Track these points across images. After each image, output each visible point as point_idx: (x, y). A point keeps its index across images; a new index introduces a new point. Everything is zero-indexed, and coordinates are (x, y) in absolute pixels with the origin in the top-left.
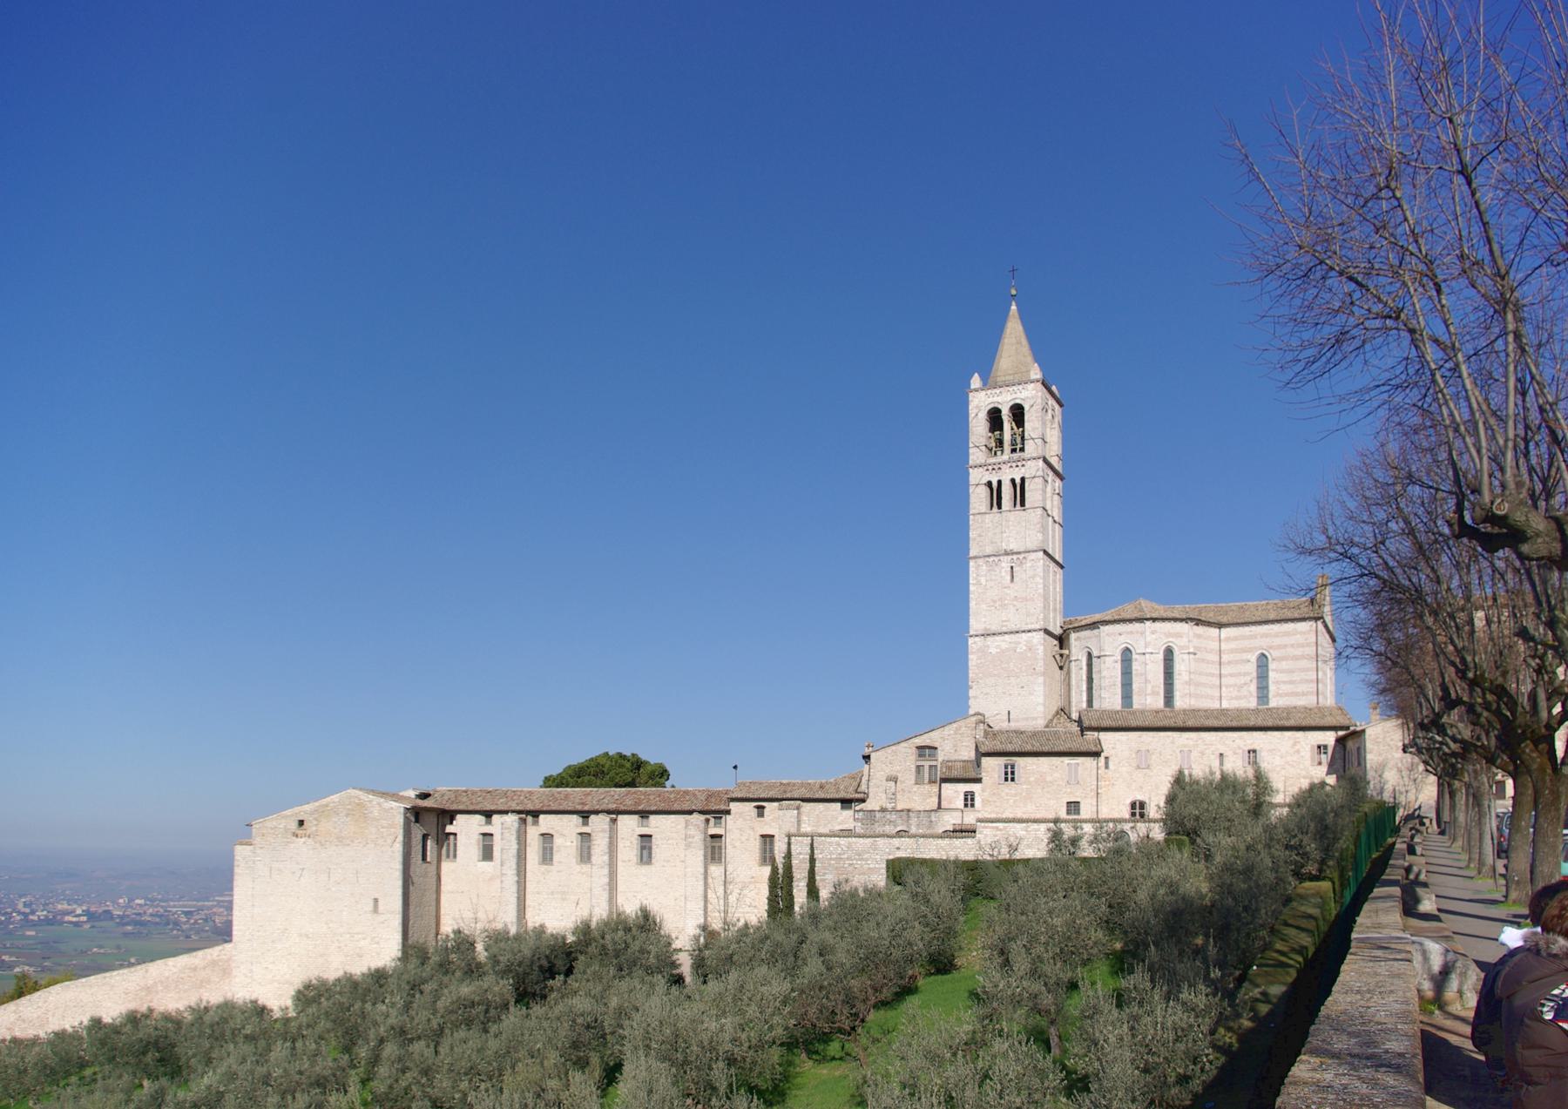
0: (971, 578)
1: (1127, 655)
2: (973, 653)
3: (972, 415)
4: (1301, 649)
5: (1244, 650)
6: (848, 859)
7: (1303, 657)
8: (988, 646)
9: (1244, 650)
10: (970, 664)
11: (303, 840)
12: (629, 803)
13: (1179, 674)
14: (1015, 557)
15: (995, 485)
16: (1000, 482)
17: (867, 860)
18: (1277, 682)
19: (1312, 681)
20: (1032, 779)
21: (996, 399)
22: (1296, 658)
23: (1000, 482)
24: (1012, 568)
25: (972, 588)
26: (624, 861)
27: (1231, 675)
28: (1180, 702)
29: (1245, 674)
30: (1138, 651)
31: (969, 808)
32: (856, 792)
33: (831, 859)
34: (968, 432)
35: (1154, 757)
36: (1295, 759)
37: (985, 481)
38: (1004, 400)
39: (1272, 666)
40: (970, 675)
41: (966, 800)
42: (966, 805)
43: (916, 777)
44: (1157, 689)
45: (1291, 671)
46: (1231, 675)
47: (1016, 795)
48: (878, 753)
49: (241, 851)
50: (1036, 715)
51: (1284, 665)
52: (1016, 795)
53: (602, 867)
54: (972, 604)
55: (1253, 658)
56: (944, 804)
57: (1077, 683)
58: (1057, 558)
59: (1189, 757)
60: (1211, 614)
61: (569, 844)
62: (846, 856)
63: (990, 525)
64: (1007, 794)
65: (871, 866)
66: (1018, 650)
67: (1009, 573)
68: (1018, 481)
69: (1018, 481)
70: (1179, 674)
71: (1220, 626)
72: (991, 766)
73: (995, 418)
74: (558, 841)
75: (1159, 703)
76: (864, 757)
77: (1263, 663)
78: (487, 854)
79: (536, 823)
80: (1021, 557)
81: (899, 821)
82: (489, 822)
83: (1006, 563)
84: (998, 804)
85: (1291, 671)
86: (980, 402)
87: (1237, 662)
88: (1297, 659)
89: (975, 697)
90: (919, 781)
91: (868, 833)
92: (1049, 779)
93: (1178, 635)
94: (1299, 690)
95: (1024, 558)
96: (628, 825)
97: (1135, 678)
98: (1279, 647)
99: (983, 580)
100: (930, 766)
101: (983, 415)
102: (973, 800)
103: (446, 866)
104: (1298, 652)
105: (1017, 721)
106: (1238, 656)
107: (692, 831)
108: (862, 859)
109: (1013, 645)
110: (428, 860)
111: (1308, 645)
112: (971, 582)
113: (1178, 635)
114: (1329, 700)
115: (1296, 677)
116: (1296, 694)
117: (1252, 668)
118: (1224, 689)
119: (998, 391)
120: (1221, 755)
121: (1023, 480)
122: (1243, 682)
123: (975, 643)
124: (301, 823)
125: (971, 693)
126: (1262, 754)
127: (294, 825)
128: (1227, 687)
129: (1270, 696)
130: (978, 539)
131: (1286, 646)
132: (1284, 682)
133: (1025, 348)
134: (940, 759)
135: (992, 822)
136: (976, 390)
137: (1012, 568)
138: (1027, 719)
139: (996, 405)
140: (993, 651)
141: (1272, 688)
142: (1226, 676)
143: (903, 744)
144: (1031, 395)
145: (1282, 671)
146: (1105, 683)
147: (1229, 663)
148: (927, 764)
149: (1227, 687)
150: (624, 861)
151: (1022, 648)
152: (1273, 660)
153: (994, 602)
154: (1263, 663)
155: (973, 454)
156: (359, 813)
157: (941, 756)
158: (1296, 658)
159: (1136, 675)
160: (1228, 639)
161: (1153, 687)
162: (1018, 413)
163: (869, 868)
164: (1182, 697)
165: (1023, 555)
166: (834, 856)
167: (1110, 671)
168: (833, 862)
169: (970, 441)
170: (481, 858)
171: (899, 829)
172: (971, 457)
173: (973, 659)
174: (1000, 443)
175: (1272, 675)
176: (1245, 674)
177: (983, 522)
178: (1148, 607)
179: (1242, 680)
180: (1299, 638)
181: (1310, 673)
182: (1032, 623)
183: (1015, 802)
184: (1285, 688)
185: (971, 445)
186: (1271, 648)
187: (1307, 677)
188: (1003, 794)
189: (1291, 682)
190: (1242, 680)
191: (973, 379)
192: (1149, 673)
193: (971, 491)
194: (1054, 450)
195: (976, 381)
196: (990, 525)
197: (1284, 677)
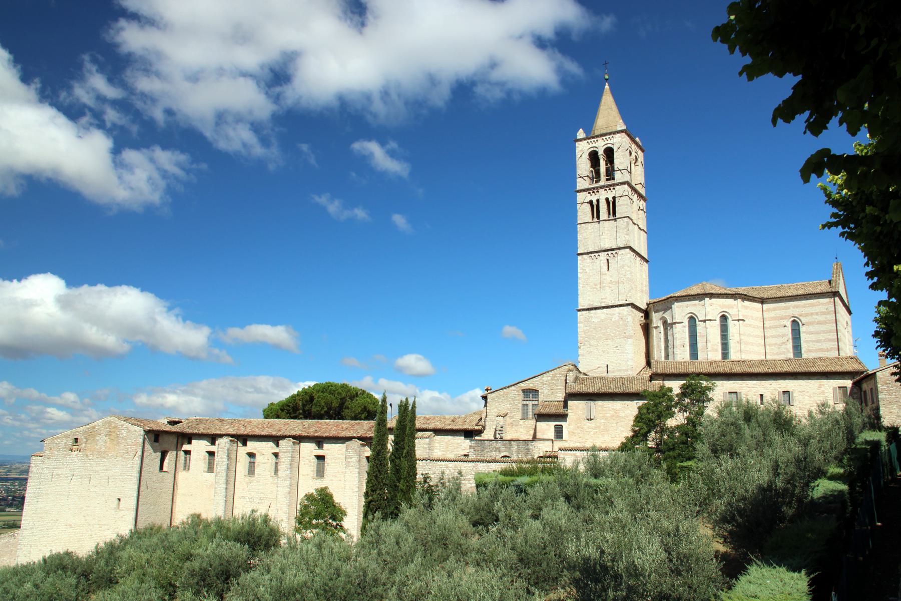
0: (579, 269)
1: (692, 320)
2: (581, 322)
3: (578, 156)
4: (824, 316)
5: (782, 318)
7: (825, 323)
8: (592, 317)
9: (782, 318)
10: (579, 330)
11: (76, 452)
12: (311, 432)
13: (733, 336)
14: (609, 253)
15: (595, 203)
16: (598, 201)
20: (608, 415)
21: (594, 145)
22: (819, 323)
23: (598, 201)
24: (608, 260)
25: (579, 275)
26: (303, 475)
27: (773, 337)
28: (733, 355)
29: (783, 336)
32: (477, 425)
34: (576, 168)
38: (600, 145)
39: (802, 329)
40: (579, 339)
44: (715, 347)
45: (818, 333)
46: (773, 337)
47: (595, 428)
48: (493, 395)
49: (35, 461)
51: (812, 328)
52: (595, 428)
53: (285, 480)
54: (580, 287)
55: (789, 324)
56: (539, 436)
57: (658, 344)
58: (643, 254)
61: (266, 461)
64: (588, 428)
66: (613, 320)
67: (606, 264)
68: (611, 199)
69: (611, 199)
70: (733, 336)
71: (762, 301)
72: (576, 408)
73: (594, 157)
74: (258, 458)
75: (718, 357)
77: (796, 325)
78: (211, 468)
79: (245, 444)
80: (614, 252)
81: (503, 449)
82: (213, 443)
84: (581, 435)
85: (818, 333)
86: (583, 149)
87: (776, 327)
88: (821, 324)
89: (583, 355)
92: (623, 415)
93: (731, 307)
95: (616, 253)
96: (309, 449)
97: (698, 339)
98: (807, 315)
99: (588, 270)
100: (533, 405)
101: (586, 156)
103: (182, 475)
104: (822, 318)
105: (613, 372)
106: (777, 322)
107: (351, 453)
110: (165, 469)
111: (829, 313)
112: (579, 271)
113: (731, 307)
114: (848, 350)
115: (822, 337)
117: (788, 331)
118: (767, 347)
119: (595, 140)
121: (614, 198)
122: (782, 341)
123: (582, 315)
124: (76, 440)
125: (580, 352)
126: (794, 395)
127: (70, 442)
128: (770, 345)
129: (803, 352)
131: (812, 314)
134: (540, 400)
135: (570, 450)
136: (581, 140)
137: (608, 260)
138: (620, 371)
139: (594, 149)
140: (595, 320)
141: (803, 345)
142: (768, 337)
143: (513, 388)
144: (620, 143)
145: (811, 333)
147: (770, 328)
149: (770, 345)
150: (303, 475)
151: (616, 318)
152: (803, 325)
153: (596, 285)
154: (796, 325)
156: (112, 433)
157: (541, 397)
158: (819, 323)
160: (768, 310)
161: (712, 345)
162: (609, 152)
164: (734, 353)
165: (615, 251)
167: (681, 333)
169: (577, 173)
170: (206, 469)
171: (503, 454)
172: (578, 184)
173: (581, 327)
174: (598, 173)
175: (803, 336)
176: (783, 336)
177: (587, 229)
178: (710, 288)
179: (780, 340)
180: (823, 309)
181: (832, 334)
183: (594, 434)
185: (578, 176)
186: (801, 315)
187: (829, 337)
188: (585, 427)
189: (818, 341)
190: (780, 340)
191: (579, 132)
192: (710, 335)
193: (578, 207)
194: (638, 176)
195: (581, 134)
197: (813, 337)
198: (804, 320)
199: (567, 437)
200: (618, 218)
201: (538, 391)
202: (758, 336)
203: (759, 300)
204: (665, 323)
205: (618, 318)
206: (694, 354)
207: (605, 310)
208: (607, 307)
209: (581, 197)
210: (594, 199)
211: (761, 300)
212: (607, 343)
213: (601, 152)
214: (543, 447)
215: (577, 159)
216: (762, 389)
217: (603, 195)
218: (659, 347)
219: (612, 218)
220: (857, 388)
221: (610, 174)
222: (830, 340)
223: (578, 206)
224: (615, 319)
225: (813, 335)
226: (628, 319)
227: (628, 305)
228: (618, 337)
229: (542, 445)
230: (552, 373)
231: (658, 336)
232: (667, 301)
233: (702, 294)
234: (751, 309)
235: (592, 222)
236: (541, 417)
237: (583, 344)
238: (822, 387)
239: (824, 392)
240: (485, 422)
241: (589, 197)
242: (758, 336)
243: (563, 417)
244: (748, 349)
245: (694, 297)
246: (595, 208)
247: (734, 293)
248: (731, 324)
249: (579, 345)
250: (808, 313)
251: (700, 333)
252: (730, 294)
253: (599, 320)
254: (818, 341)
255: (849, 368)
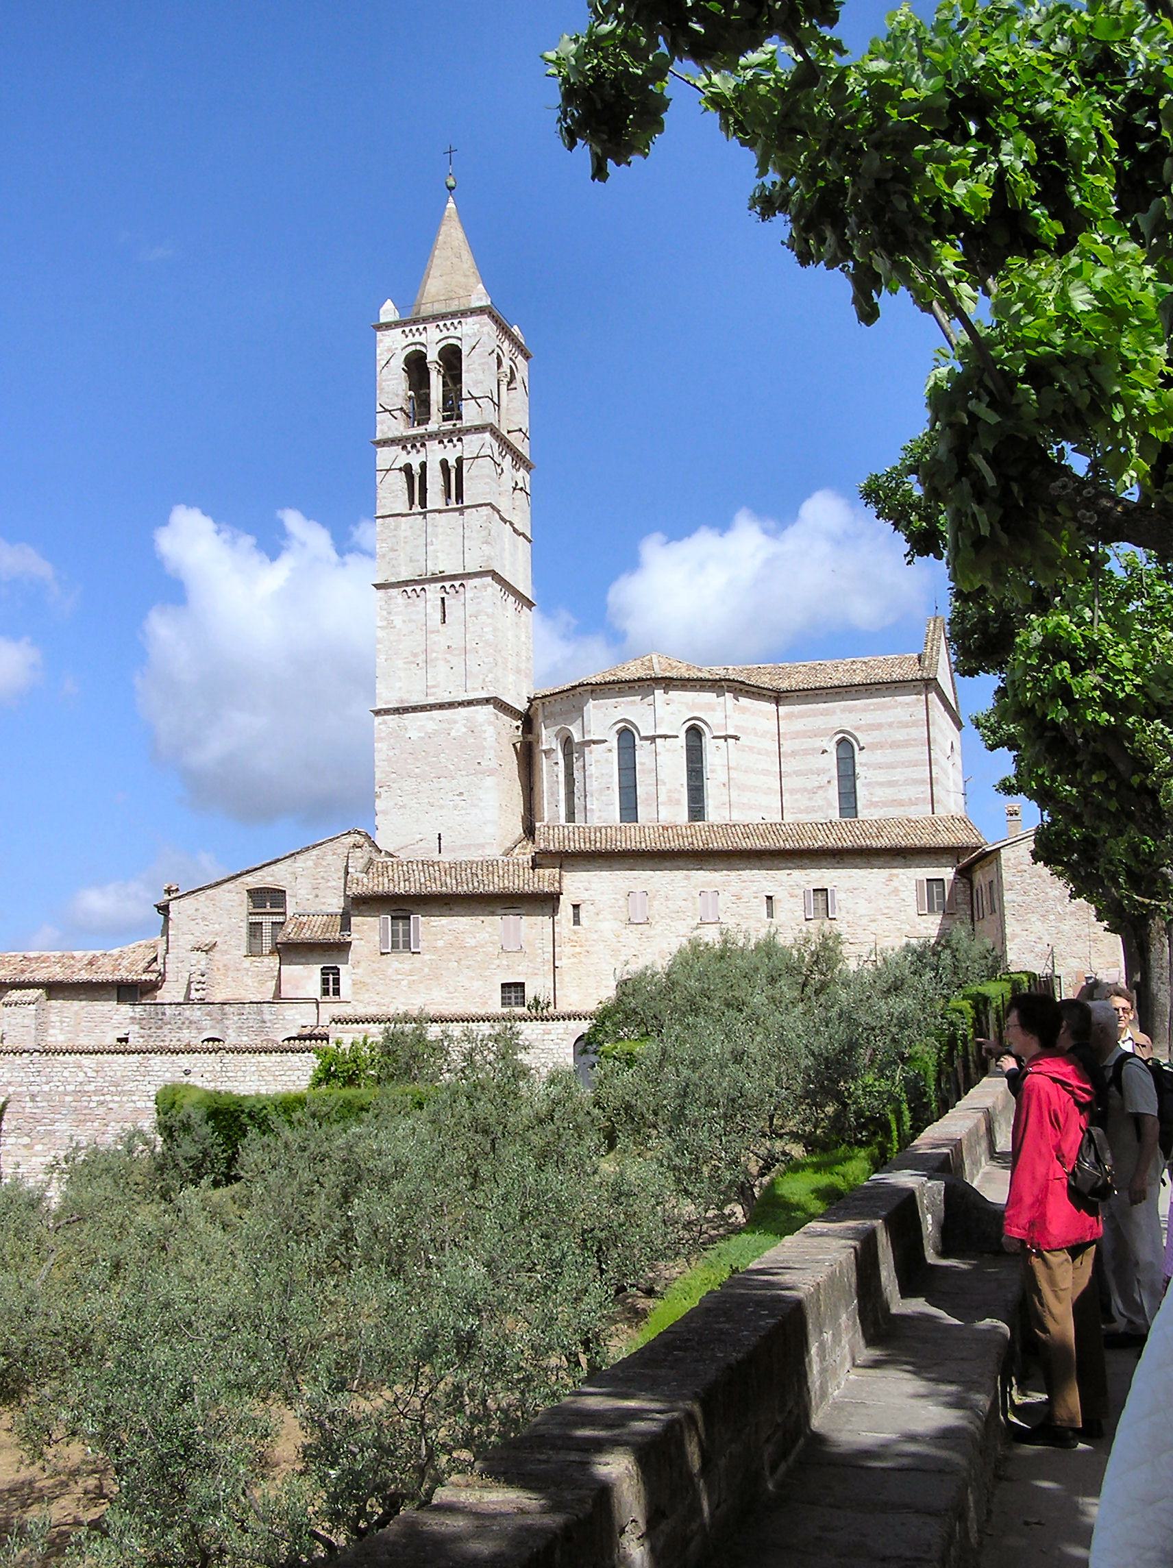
1: (627, 736)
2: (381, 739)
5: (816, 734)
6: (95, 1092)
9: (816, 734)
14: (447, 584)
15: (416, 469)
16: (423, 466)
17: (131, 1093)
18: (869, 784)
19: (922, 782)
21: (418, 338)
22: (895, 745)
23: (423, 466)
24: (443, 599)
27: (798, 773)
30: (642, 734)
31: (331, 997)
32: (146, 971)
33: (66, 1094)
35: (656, 903)
36: (891, 904)
37: (400, 464)
38: (432, 341)
39: (859, 757)
40: (377, 776)
41: (325, 982)
42: (325, 992)
43: (250, 944)
44: (676, 796)
45: (891, 766)
46: (798, 773)
50: (482, 841)
51: (878, 756)
55: (832, 747)
56: (286, 991)
57: (551, 788)
59: (716, 903)
60: (766, 679)
62: (91, 1087)
63: (408, 533)
65: (139, 1104)
66: (453, 733)
68: (452, 463)
69: (452, 463)
70: (712, 771)
71: (778, 697)
73: (416, 365)
76: (159, 908)
77: (846, 747)
81: (207, 1023)
83: (433, 591)
84: (380, 988)
85: (891, 766)
87: (806, 752)
89: (385, 812)
90: (253, 952)
91: (151, 1044)
92: (471, 942)
94: (904, 796)
99: (398, 621)
101: (398, 363)
102: (336, 981)
104: (900, 735)
108: (119, 1093)
109: (446, 725)
111: (915, 724)
113: (710, 708)
114: (952, 803)
115: (898, 775)
116: (900, 803)
117: (831, 761)
119: (421, 327)
120: (769, 898)
121: (460, 461)
125: (379, 805)
126: (837, 896)
130: (391, 555)
132: (881, 784)
133: (467, 261)
134: (290, 913)
136: (388, 326)
137: (443, 599)
139: (419, 347)
140: (414, 735)
142: (789, 775)
146: (593, 785)
147: (794, 754)
148: (267, 920)
151: (459, 730)
152: (862, 749)
153: (415, 655)
154: (846, 747)
155: (383, 422)
158: (895, 745)
159: (643, 771)
160: (790, 716)
162: (452, 358)
163: (136, 1110)
166: (70, 1088)
168: (69, 1099)
179: (814, 781)
182: (475, 689)
184: (881, 794)
186: (857, 729)
189: (891, 784)
193: (378, 479)
195: (388, 312)
196: (408, 533)
197: (881, 776)
198: (863, 739)
199: (350, 992)
200: (468, 507)
201: (284, 892)
202: (766, 772)
203: (770, 693)
204: (567, 742)
205: (464, 730)
206: (629, 809)
207: (435, 713)
208: (441, 706)
209: (385, 456)
210: (415, 460)
211: (775, 694)
212: (441, 785)
213: (432, 356)
214: (296, 1017)
215: (378, 369)
216: (771, 884)
217: (435, 453)
218: (554, 794)
219: (456, 506)
220: (965, 880)
221: (452, 409)
222: (916, 782)
223: (379, 476)
224: (458, 731)
225: (882, 771)
226: (485, 732)
227: (487, 701)
228: (464, 773)
229: (294, 1011)
230: (315, 852)
231: (551, 773)
232: (572, 692)
233: (647, 679)
234: (754, 714)
235: (409, 515)
236: (291, 951)
237: (386, 788)
238: (895, 878)
239: (898, 890)
240: (164, 963)
241: (403, 458)
242: (766, 772)
243: (342, 948)
244: (745, 801)
245: (631, 685)
246: (416, 482)
247: (717, 677)
248: (709, 744)
249: (377, 789)
250: (873, 725)
251: (644, 764)
252: (709, 680)
253: (422, 735)
254: (891, 784)
255: (945, 839)
